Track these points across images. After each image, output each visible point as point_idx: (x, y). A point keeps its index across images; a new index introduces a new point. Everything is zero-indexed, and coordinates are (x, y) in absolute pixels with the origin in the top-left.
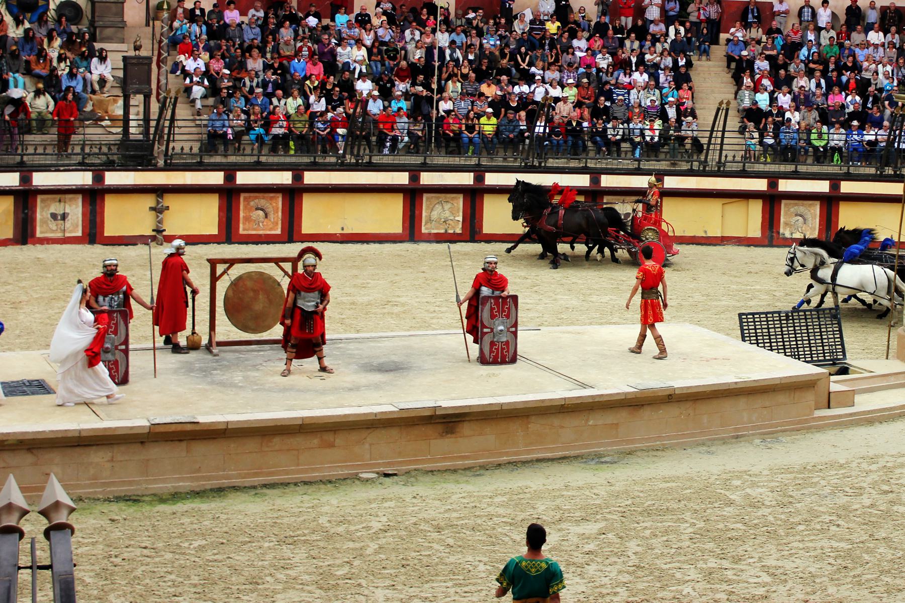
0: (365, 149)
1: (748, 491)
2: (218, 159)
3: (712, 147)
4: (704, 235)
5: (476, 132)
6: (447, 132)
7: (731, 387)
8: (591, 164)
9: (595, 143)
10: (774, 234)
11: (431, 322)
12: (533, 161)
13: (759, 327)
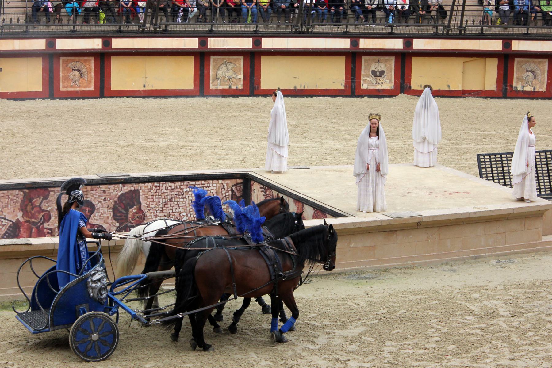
0: (161, 19)
1: (485, 302)
2: (41, 29)
3: (454, 13)
4: (448, 89)
5: (254, 4)
6: (230, 4)
7: (471, 216)
8: (351, 30)
9: (354, 11)
10: (508, 88)
11: (219, 162)
12: (302, 28)
13: (495, 166)
